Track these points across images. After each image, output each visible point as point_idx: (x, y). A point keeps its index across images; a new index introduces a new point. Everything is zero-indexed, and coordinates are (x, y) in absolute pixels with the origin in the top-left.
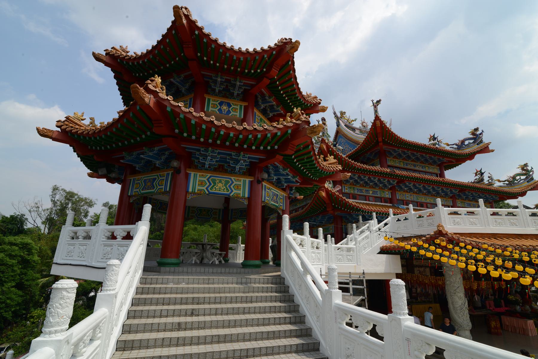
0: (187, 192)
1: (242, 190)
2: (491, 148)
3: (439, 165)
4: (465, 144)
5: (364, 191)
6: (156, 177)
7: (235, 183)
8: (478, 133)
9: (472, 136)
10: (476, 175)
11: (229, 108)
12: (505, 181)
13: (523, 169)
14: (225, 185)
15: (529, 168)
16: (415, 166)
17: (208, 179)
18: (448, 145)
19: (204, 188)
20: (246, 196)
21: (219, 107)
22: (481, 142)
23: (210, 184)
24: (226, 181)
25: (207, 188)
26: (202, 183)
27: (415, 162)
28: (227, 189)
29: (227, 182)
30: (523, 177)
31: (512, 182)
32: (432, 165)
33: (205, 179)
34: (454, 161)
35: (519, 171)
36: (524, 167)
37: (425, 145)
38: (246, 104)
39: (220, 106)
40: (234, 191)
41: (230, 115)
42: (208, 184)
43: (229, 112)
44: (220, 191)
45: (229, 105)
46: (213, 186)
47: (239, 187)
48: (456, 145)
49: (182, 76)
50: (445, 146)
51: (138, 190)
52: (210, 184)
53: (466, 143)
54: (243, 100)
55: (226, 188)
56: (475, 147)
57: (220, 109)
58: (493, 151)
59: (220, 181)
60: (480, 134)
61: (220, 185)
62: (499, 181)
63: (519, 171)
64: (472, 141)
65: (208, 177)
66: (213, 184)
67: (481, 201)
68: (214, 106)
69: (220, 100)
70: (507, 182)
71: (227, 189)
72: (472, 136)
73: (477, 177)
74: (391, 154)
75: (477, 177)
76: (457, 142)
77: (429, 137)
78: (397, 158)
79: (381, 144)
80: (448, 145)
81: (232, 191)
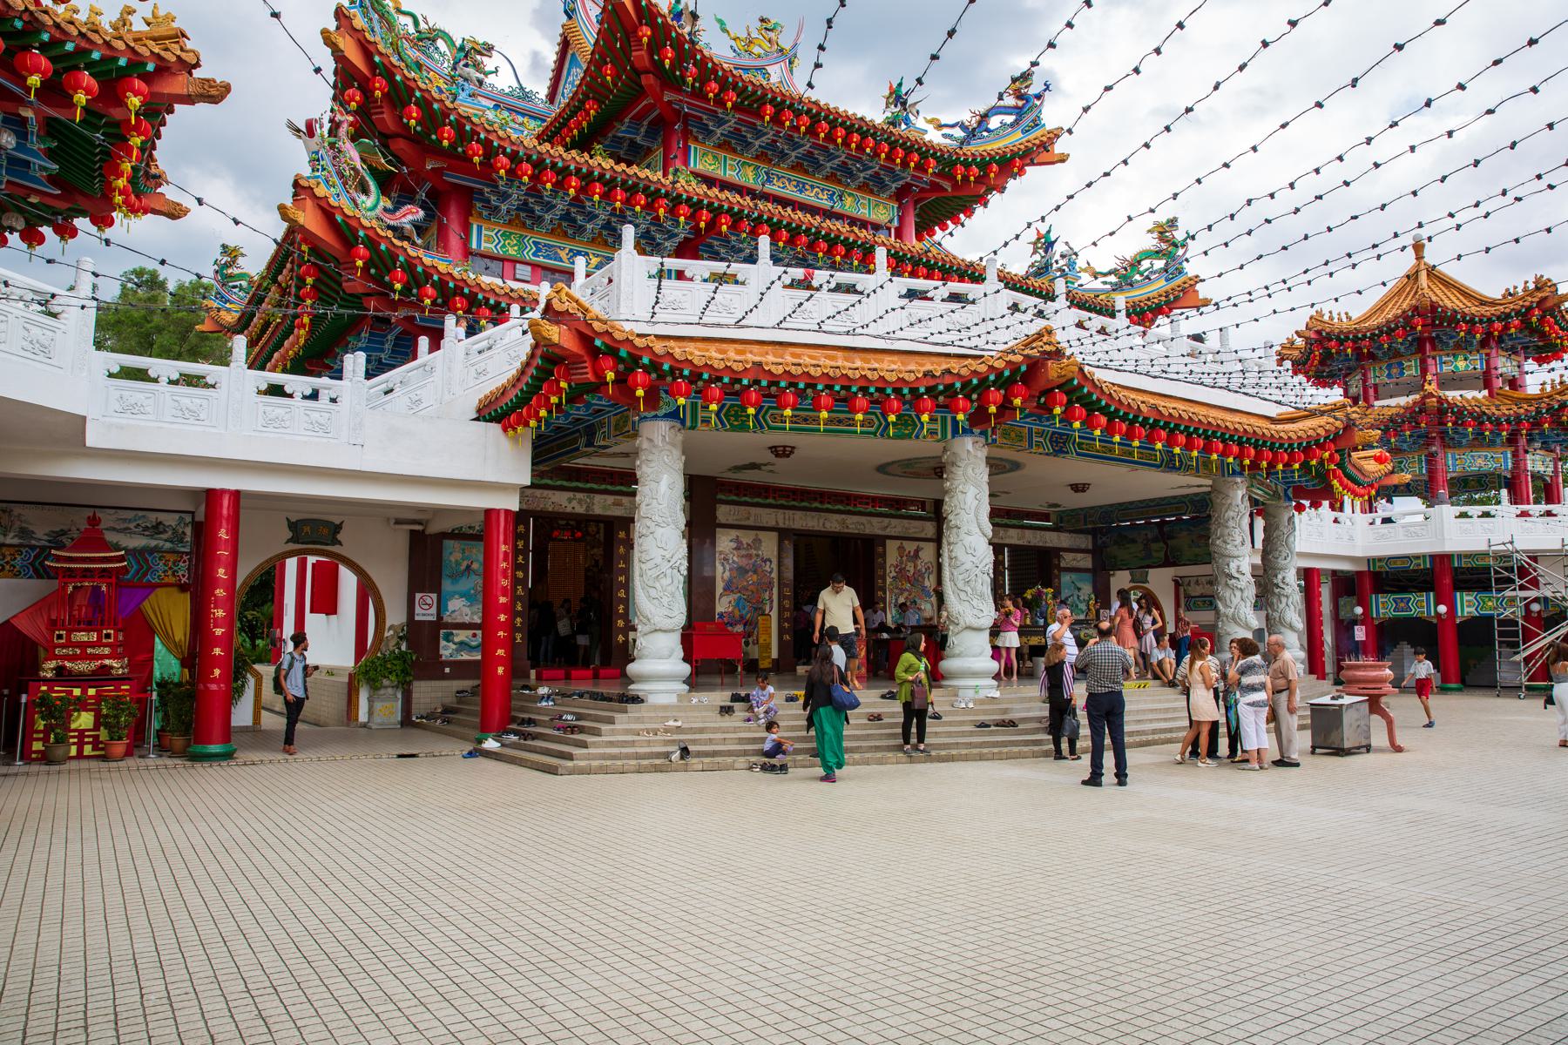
2: (1059, 147)
3: (899, 195)
4: (991, 127)
5: (563, 254)
8: (1032, 91)
9: (1010, 101)
10: (1035, 252)
12: (1105, 275)
13: (1162, 239)
15: (1179, 235)
16: (801, 187)
18: (940, 126)
22: (1036, 123)
27: (806, 172)
30: (1159, 264)
31: (1126, 275)
32: (871, 192)
34: (947, 186)
35: (1151, 242)
36: (1164, 231)
37: (816, 103)
48: (962, 126)
50: (930, 128)
53: (994, 122)
56: (1016, 139)
58: (1063, 159)
60: (1038, 97)
62: (1095, 275)
63: (1151, 242)
64: (1010, 119)
67: (764, 242)
70: (1113, 279)
72: (1010, 101)
73: (1037, 257)
74: (709, 133)
75: (1037, 257)
76: (966, 117)
77: (887, 93)
78: (734, 151)
79: (648, 80)
80: (940, 126)
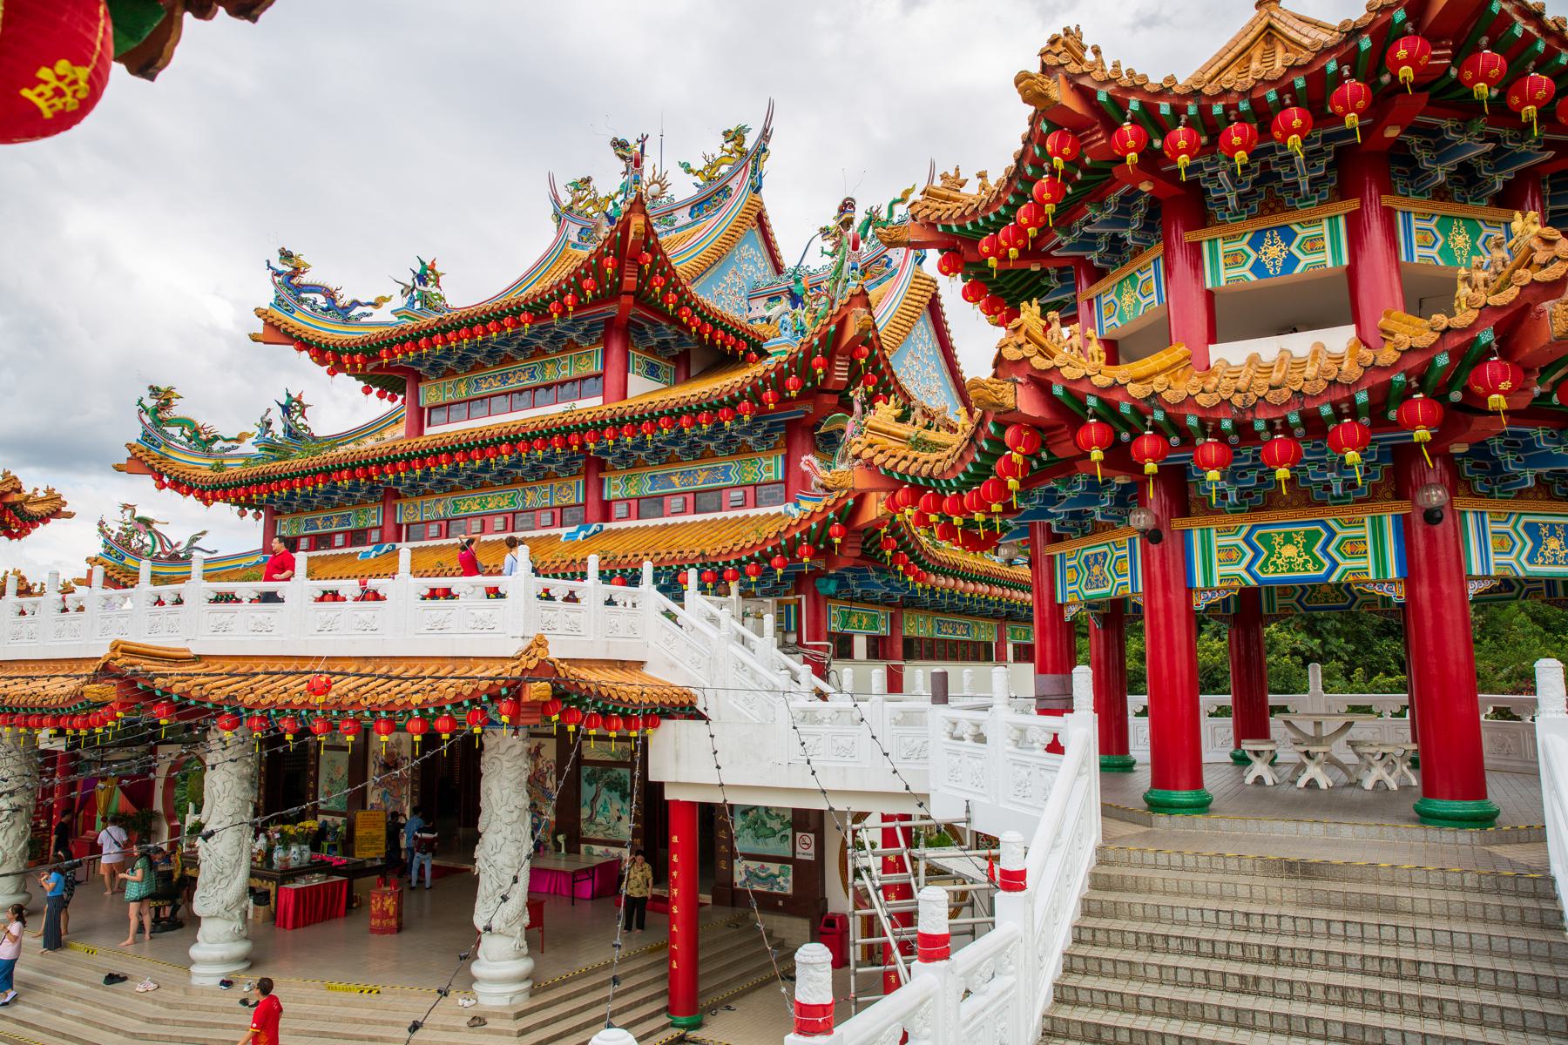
0: (1189, 591)
1: (1370, 554)
6: (1105, 549)
7: (1342, 533)
11: (1289, 244)
14: (1308, 549)
17: (1246, 540)
19: (1239, 569)
20: (1393, 573)
21: (1254, 256)
23: (1257, 554)
24: (1307, 535)
25: (1248, 569)
26: (1230, 555)
28: (1316, 560)
29: (1311, 538)
33: (1237, 540)
38: (1353, 205)
39: (1257, 250)
40: (1344, 564)
41: (1298, 270)
42: (1250, 554)
43: (1292, 261)
44: (1291, 570)
45: (1288, 236)
46: (1268, 559)
47: (1361, 548)
49: (1112, 199)
51: (1075, 588)
52: (1257, 554)
54: (1342, 194)
55: (1313, 556)
57: (1258, 260)
59: (1288, 539)
61: (1289, 551)
65: (1245, 531)
66: (1266, 553)
68: (1235, 259)
69: (1252, 227)
71: (1316, 560)
81: (1335, 565)
